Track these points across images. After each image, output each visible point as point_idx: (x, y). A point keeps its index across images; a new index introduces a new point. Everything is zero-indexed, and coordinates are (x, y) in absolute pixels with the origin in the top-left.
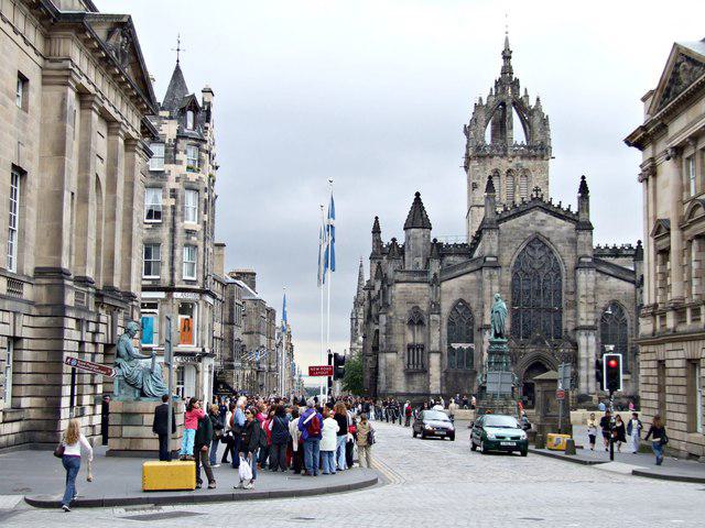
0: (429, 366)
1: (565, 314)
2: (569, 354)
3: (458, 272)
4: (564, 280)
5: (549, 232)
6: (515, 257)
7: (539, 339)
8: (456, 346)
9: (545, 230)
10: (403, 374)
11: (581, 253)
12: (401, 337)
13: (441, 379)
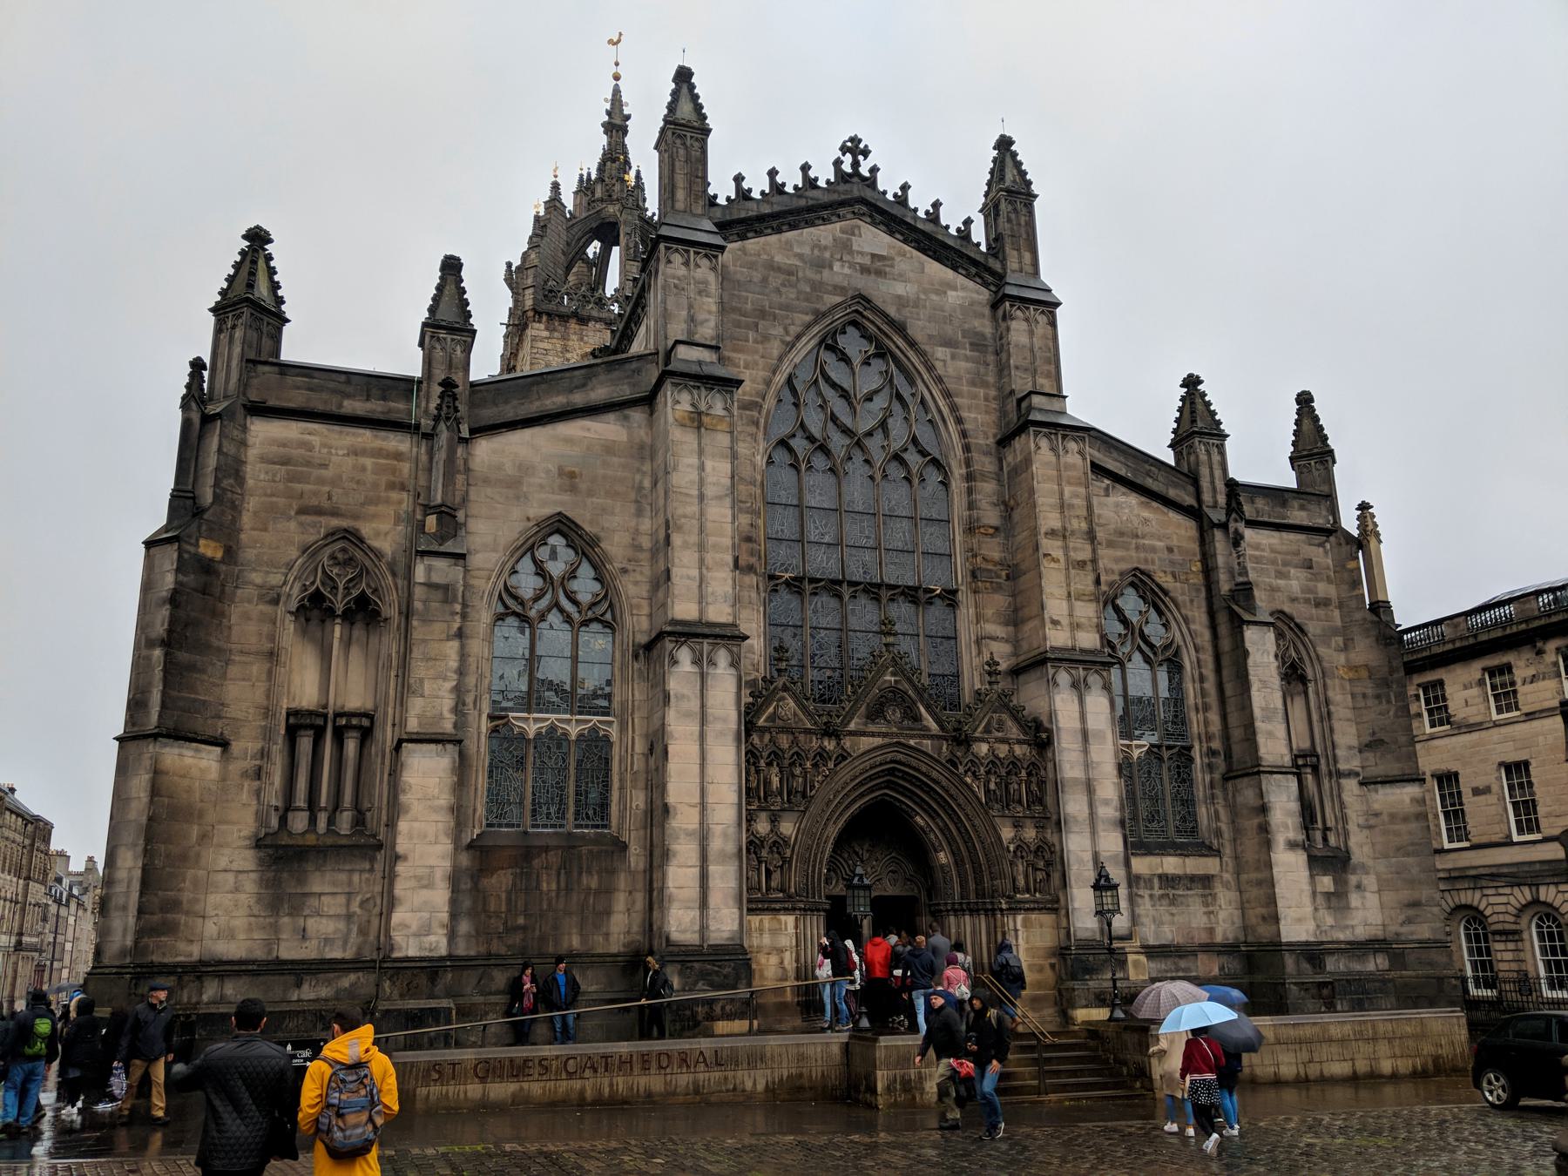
0: (395, 809)
1: (966, 612)
2: (1014, 764)
3: (556, 401)
4: (958, 485)
5: (901, 301)
6: (780, 379)
7: (894, 695)
8: (532, 725)
9: (886, 292)
10: (246, 859)
11: (1021, 383)
12: (257, 669)
13: (454, 880)
